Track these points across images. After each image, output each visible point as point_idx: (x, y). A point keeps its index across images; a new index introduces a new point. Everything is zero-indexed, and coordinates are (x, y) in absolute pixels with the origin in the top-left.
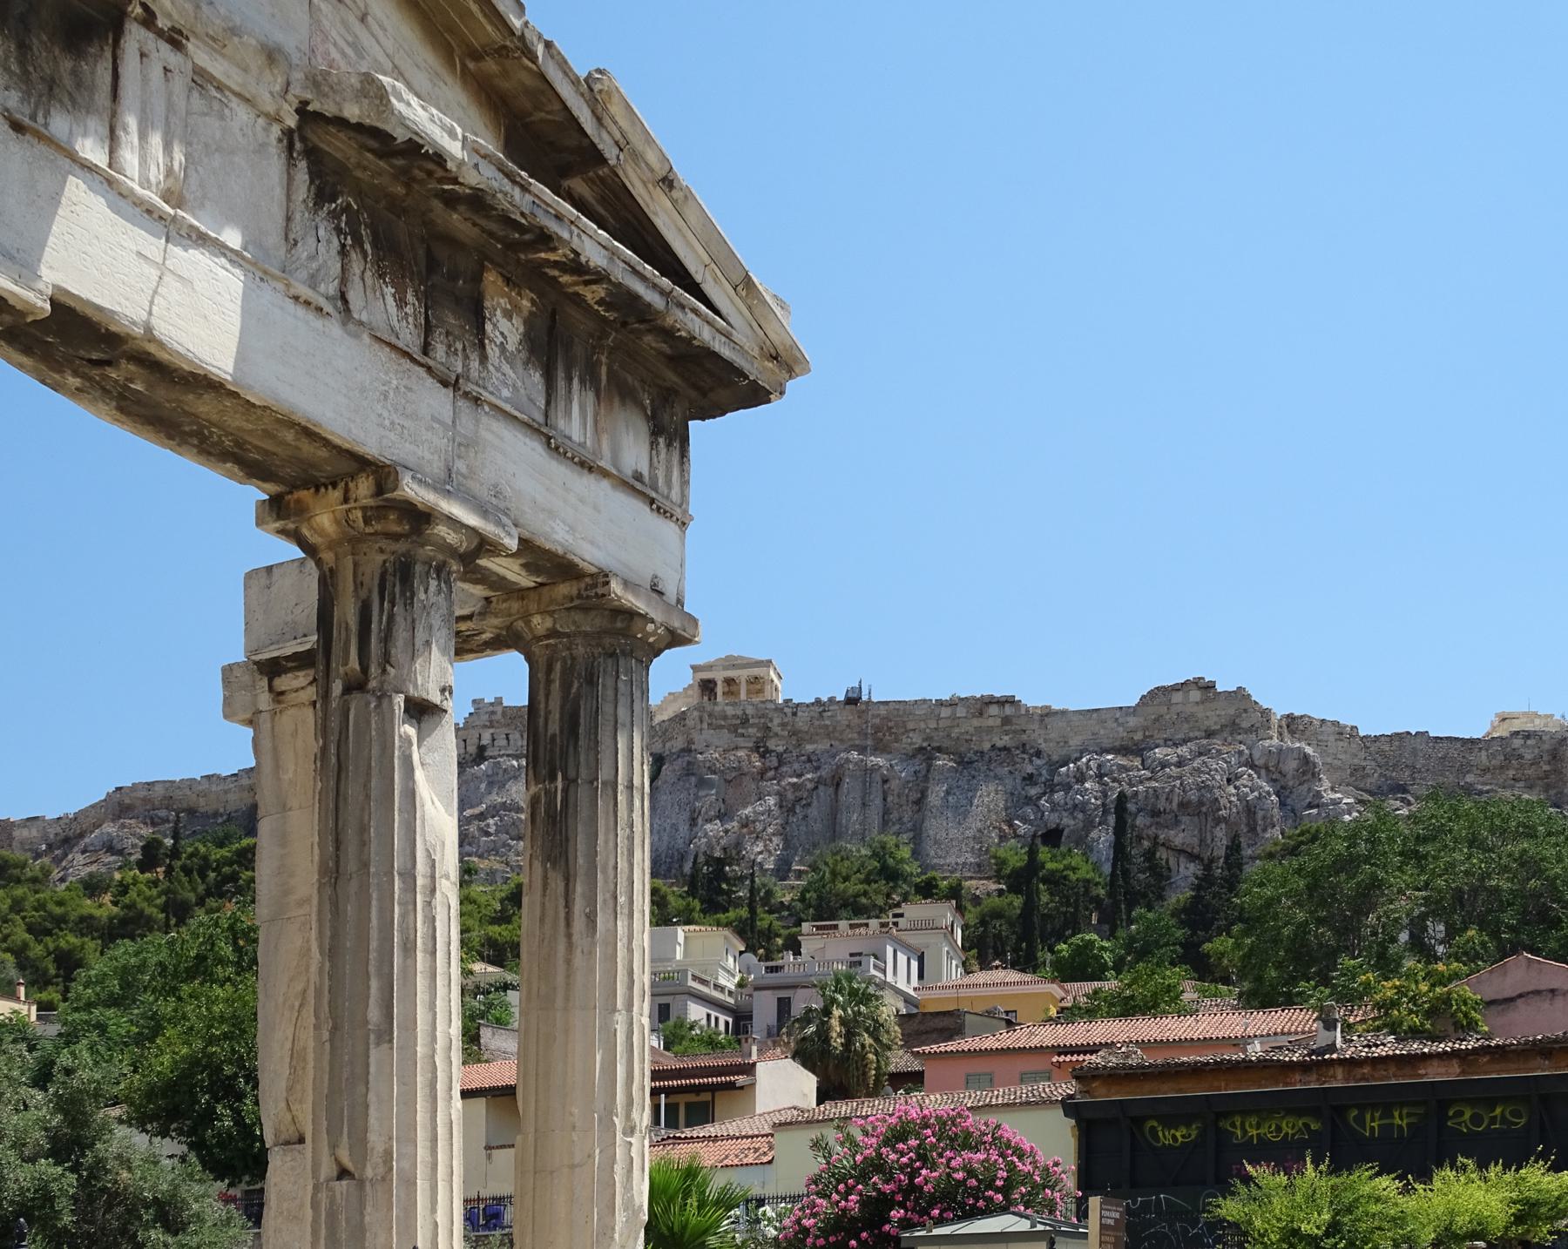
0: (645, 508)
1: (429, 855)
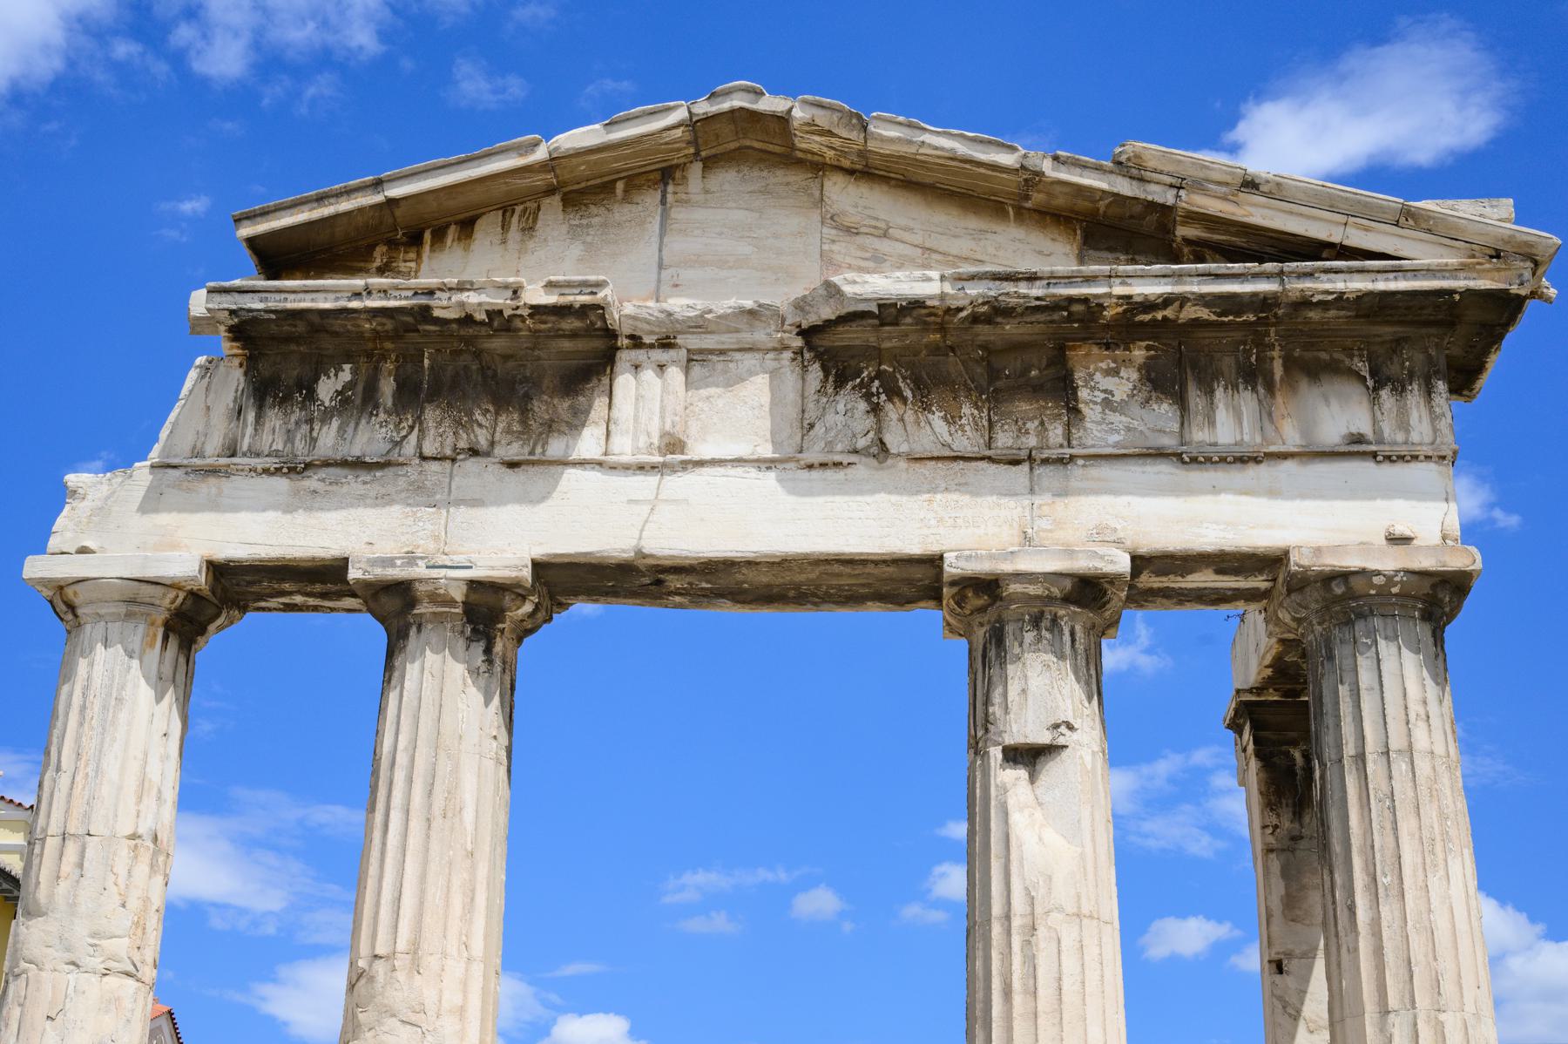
0: (1368, 466)
1: (1028, 893)
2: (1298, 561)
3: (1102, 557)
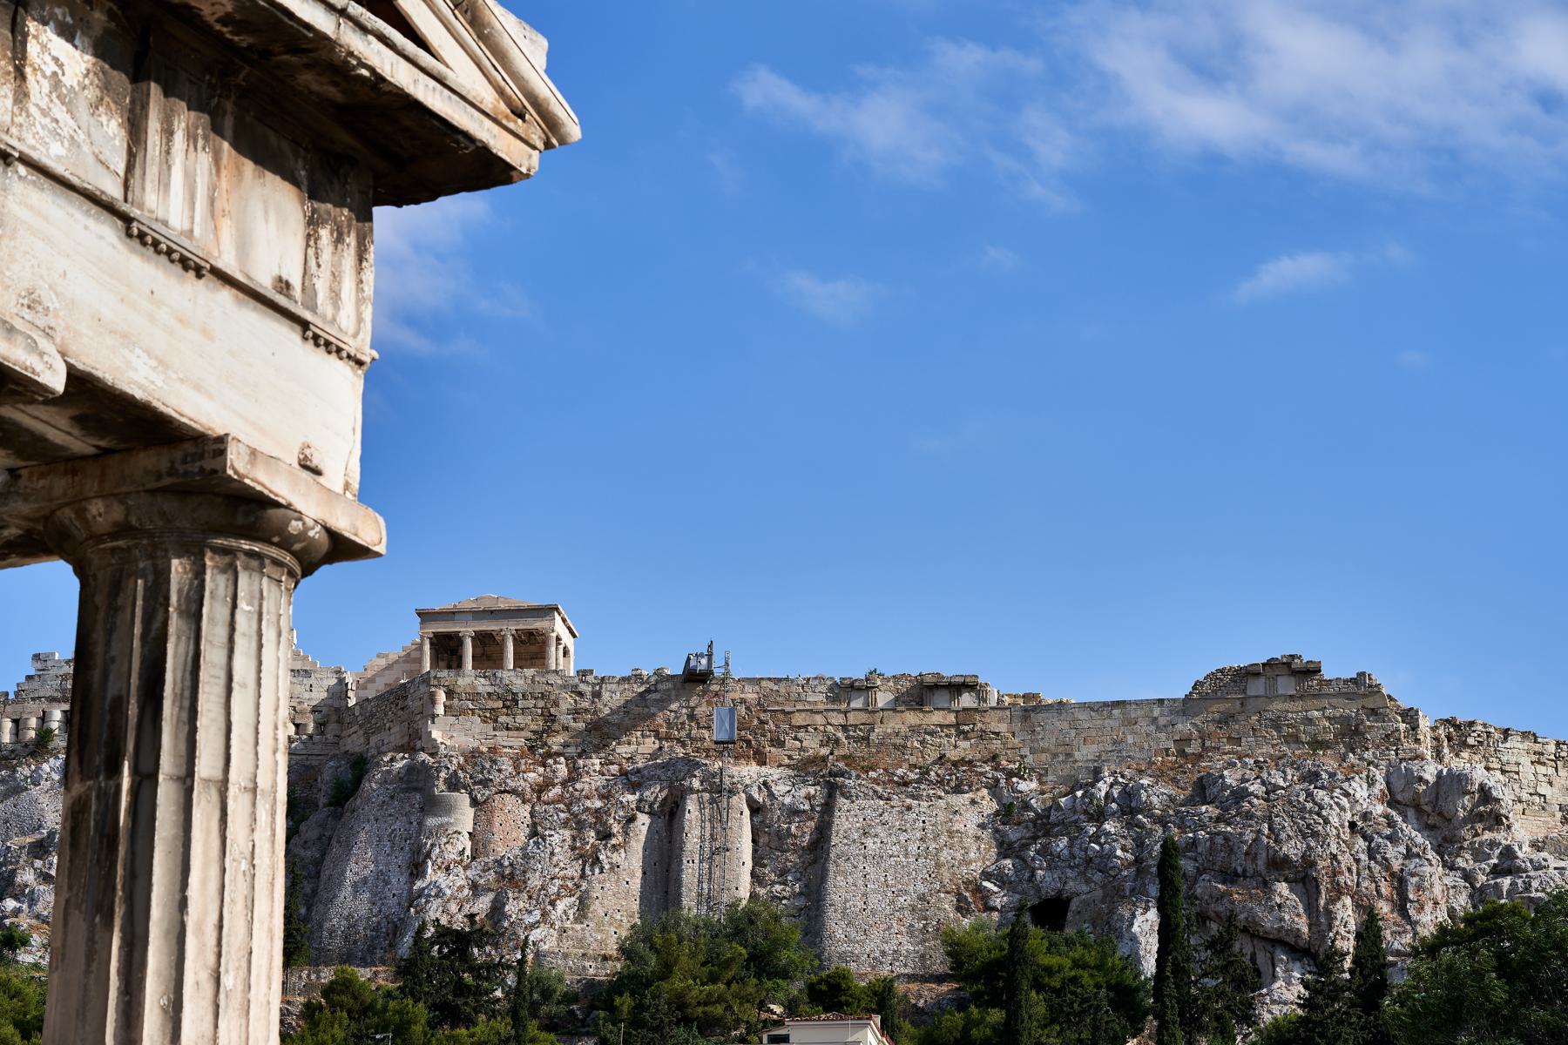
2: (236, 462)
3: (42, 354)
